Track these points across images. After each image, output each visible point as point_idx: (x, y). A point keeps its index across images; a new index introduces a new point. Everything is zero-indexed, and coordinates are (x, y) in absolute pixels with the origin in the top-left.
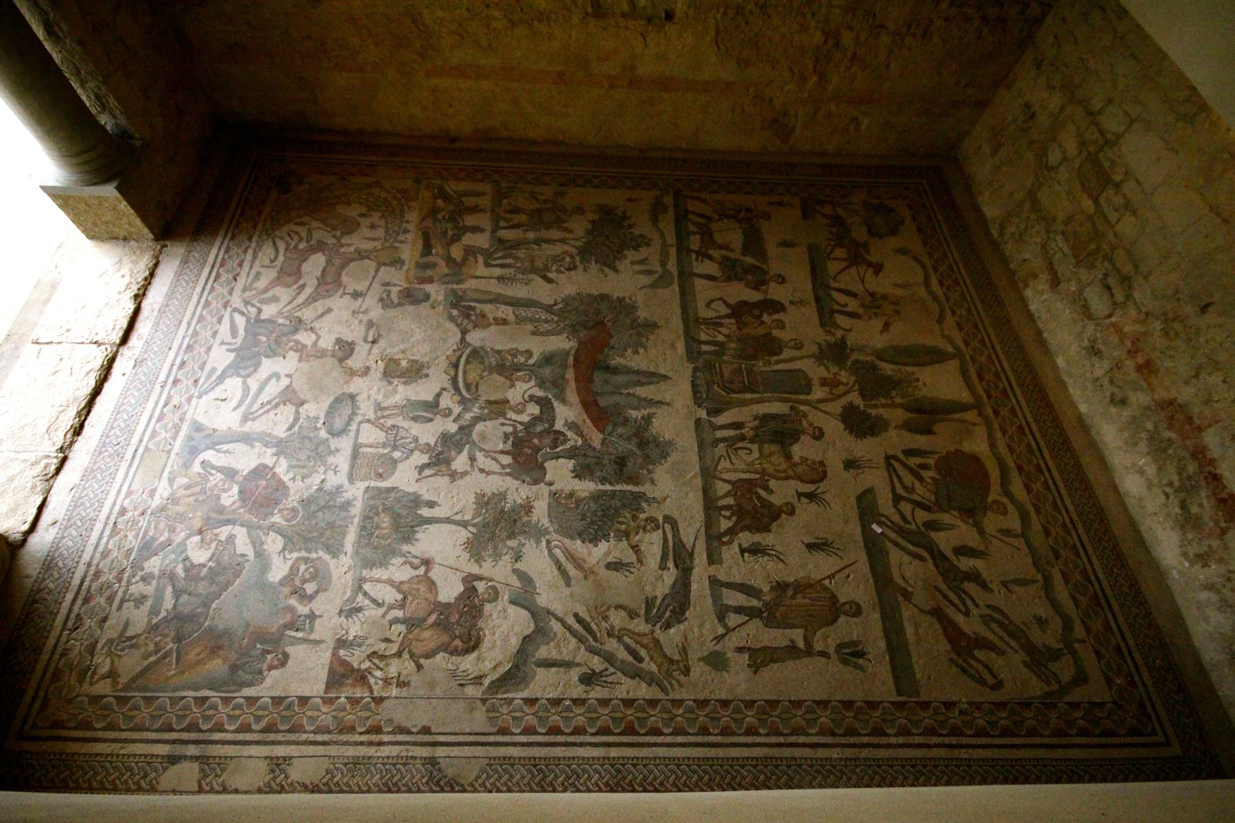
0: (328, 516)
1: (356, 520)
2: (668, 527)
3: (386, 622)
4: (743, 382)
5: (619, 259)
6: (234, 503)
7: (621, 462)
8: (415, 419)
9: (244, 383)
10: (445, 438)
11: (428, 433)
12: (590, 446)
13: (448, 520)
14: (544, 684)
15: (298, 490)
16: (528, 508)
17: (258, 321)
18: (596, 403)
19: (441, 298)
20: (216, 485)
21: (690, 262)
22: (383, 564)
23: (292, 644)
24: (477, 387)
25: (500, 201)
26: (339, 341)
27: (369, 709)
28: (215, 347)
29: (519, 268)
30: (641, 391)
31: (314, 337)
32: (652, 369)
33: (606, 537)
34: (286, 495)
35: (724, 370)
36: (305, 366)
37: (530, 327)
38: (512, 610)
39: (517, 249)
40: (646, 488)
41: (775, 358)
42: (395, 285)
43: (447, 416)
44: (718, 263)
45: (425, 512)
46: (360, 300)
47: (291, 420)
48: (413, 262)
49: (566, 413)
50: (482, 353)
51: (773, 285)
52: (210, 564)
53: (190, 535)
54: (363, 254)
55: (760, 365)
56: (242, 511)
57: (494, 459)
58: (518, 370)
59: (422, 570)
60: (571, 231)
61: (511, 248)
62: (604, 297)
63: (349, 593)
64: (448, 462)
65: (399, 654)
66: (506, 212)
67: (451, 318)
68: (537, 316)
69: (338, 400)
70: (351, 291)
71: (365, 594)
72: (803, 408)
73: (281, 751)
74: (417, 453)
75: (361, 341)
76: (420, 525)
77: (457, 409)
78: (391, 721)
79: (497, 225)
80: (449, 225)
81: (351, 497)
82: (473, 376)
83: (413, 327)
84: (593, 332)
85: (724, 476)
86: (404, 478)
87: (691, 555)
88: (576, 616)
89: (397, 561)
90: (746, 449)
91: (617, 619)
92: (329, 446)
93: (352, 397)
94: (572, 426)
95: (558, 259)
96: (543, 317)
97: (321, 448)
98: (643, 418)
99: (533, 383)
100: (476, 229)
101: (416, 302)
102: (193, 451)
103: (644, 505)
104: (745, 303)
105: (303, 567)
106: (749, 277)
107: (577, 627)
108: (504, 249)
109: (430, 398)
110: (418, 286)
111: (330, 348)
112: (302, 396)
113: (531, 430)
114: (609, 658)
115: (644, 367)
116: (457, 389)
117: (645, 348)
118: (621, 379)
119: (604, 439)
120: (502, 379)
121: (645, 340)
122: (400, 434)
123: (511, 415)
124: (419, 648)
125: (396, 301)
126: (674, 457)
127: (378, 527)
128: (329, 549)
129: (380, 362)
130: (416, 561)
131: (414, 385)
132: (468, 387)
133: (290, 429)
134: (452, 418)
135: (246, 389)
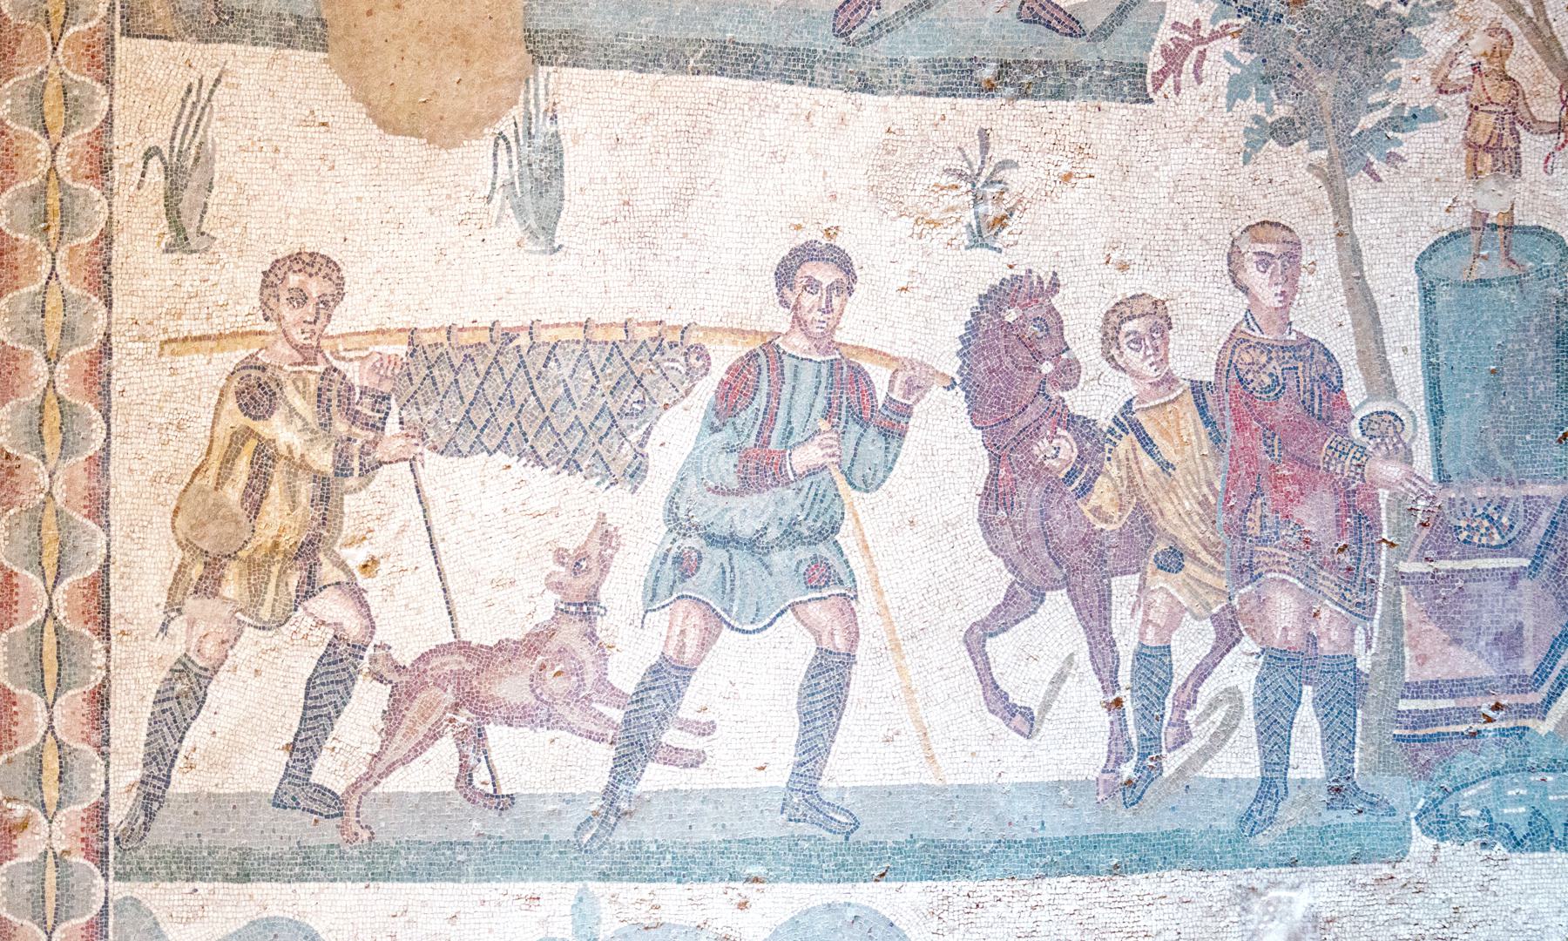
4: (1515, 577)
21: (711, 797)
35: (1428, 674)
41: (1355, 389)
104: (995, 496)
106: (805, 457)
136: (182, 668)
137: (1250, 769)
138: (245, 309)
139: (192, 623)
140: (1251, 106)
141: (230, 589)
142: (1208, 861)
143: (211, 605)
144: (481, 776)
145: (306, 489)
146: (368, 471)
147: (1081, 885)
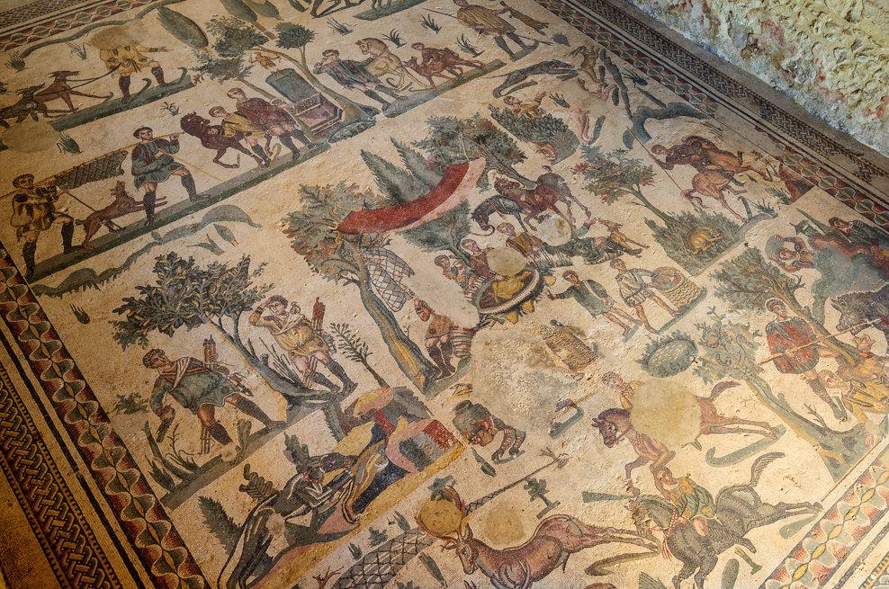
0: (743, 281)
1: (722, 260)
2: (503, 93)
3: (746, 188)
5: (223, 270)
6: (826, 356)
7: (481, 140)
8: (604, 294)
9: (754, 481)
10: (593, 257)
11: (605, 274)
12: (488, 164)
13: (648, 205)
14: (669, 97)
15: (761, 320)
16: (581, 168)
17: (689, 563)
18: (442, 183)
19: (449, 392)
20: (837, 386)
22: (721, 218)
23: (823, 225)
24: (518, 275)
25: (207, 467)
26: (610, 441)
27: (787, 159)
28: (769, 574)
29: (327, 353)
30: (398, 162)
31: (635, 473)
32: (364, 166)
33: (549, 117)
34: (771, 324)
36: (671, 442)
37: (406, 281)
38: (653, 134)
39: (296, 378)
40: (486, 114)
41: (267, 100)
42: (479, 459)
43: (572, 273)
44: (155, 185)
45: (661, 223)
46: (539, 477)
47: (726, 392)
48: (424, 474)
49: (472, 194)
50: (479, 298)
51: (155, 135)
52: (869, 323)
53: (880, 359)
54: (469, 551)
55: (287, 104)
56: (821, 344)
57: (569, 212)
58: (468, 257)
59: (694, 194)
60: (209, 343)
61: (297, 384)
62: (299, 248)
63: (761, 223)
64: (609, 240)
65: (748, 168)
66: (225, 439)
67: (466, 359)
68: (385, 285)
69: (664, 372)
70: (539, 501)
71: (749, 213)
72: (311, 68)
73: (859, 181)
74: (628, 267)
75: (584, 419)
76: (672, 219)
77: (559, 271)
78: (777, 146)
79: (265, 431)
80: (316, 491)
81: (714, 280)
82: (512, 285)
83: (515, 384)
84: (361, 229)
85: (428, 83)
86: (656, 257)
87: (510, 74)
88: (616, 103)
89: (710, 213)
90: (388, 82)
91: (594, 87)
92: (704, 337)
93: (645, 363)
94: (482, 183)
95: (274, 325)
96: (381, 279)
97: (713, 340)
98: (424, 148)
99: (469, 237)
100: (295, 452)
101: (480, 412)
102: (849, 440)
103: (501, 111)
105: (788, 263)
107: (621, 99)
108: (305, 389)
109: (572, 300)
110: (456, 434)
111: (626, 441)
112: (698, 408)
113: (517, 207)
114: (619, 79)
115: (368, 172)
116: (540, 287)
117: (342, 183)
118: (397, 180)
119: (471, 159)
120: (491, 262)
121: (332, 188)
122: (629, 292)
123: (518, 230)
124: (735, 162)
125: (500, 435)
126: (441, 115)
127: (707, 243)
128: (759, 259)
129: (587, 376)
130: (696, 202)
131: (575, 325)
132: (527, 281)
133: (732, 384)
134: (570, 268)
135: (757, 469)
136: (27, 244)
137: (289, 151)
138: (12, 188)
139: (25, 237)
140: (217, 79)
141: (32, 227)
142: (290, 165)
143: (29, 232)
144: (115, 228)
145: (42, 207)
146: (57, 198)
147: (266, 182)
